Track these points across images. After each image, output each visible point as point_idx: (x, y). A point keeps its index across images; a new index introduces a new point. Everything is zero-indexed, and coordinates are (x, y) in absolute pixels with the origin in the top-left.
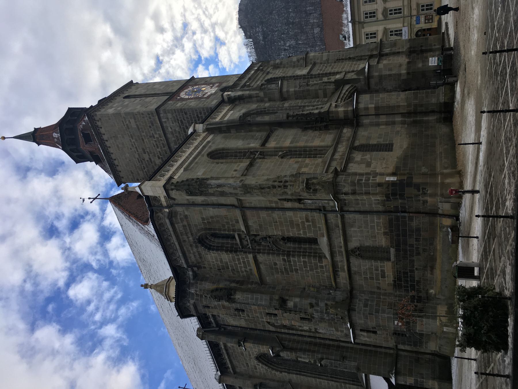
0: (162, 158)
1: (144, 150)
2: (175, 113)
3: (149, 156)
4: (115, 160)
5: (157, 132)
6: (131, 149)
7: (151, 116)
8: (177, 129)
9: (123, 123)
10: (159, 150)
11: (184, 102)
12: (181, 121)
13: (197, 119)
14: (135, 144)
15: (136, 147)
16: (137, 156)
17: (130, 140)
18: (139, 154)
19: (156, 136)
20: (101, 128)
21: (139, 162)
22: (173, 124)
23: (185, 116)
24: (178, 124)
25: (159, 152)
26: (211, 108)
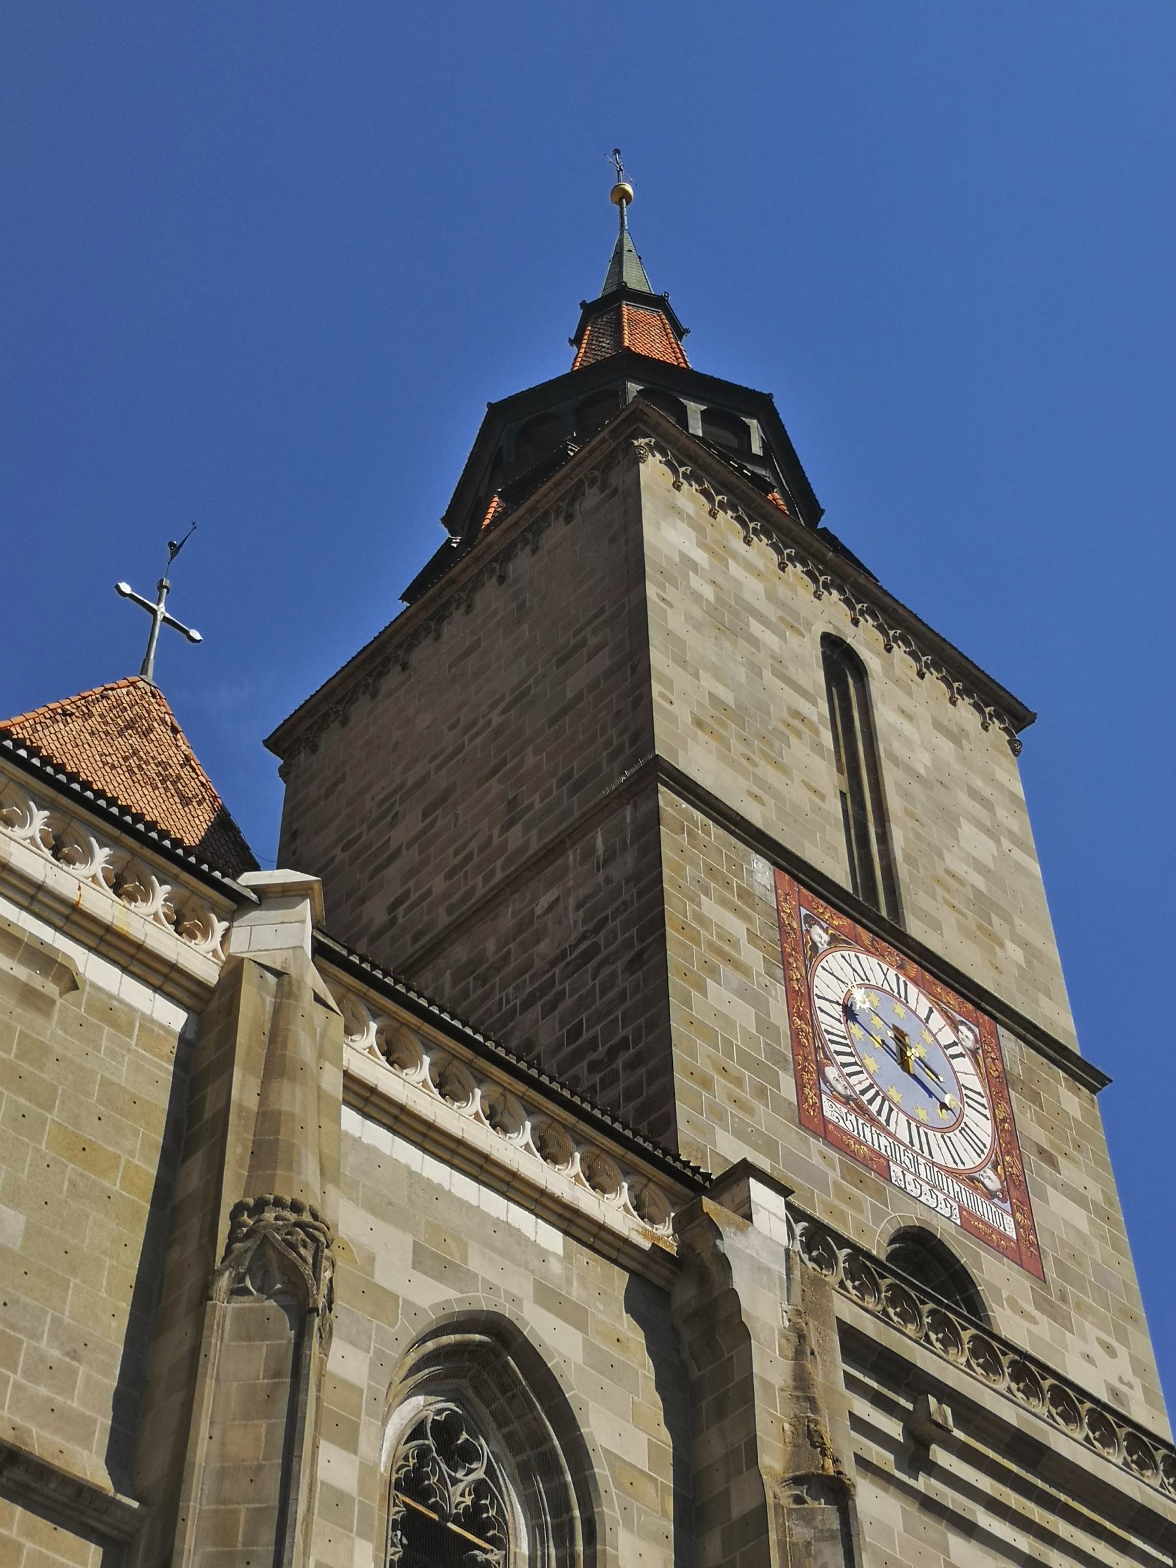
0: (393, 922)
1: (443, 798)
2: (640, 895)
3: (410, 845)
4: (404, 667)
5: (534, 832)
6: (452, 727)
7: (628, 752)
8: (544, 946)
9: (589, 622)
10: (439, 885)
11: (753, 957)
12: (594, 950)
13: (602, 1050)
14: (477, 734)
15: (461, 748)
16: (412, 777)
17: (503, 698)
18: (426, 778)
19: (517, 829)
20: (569, 518)
21: (382, 802)
22: (578, 907)
23: (619, 965)
24: (573, 938)
25: (429, 893)
26: (669, 1121)
